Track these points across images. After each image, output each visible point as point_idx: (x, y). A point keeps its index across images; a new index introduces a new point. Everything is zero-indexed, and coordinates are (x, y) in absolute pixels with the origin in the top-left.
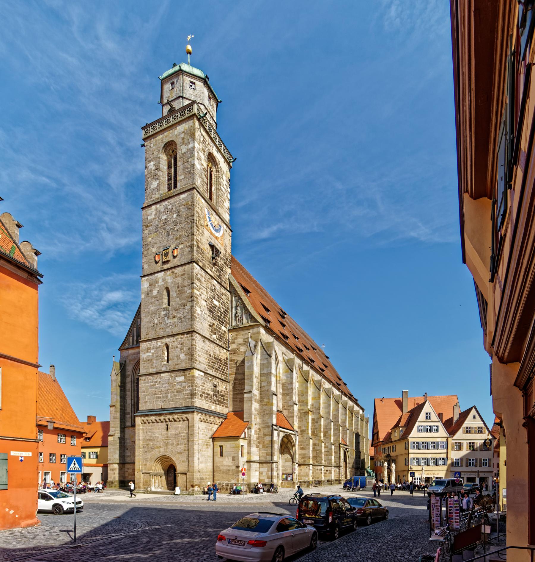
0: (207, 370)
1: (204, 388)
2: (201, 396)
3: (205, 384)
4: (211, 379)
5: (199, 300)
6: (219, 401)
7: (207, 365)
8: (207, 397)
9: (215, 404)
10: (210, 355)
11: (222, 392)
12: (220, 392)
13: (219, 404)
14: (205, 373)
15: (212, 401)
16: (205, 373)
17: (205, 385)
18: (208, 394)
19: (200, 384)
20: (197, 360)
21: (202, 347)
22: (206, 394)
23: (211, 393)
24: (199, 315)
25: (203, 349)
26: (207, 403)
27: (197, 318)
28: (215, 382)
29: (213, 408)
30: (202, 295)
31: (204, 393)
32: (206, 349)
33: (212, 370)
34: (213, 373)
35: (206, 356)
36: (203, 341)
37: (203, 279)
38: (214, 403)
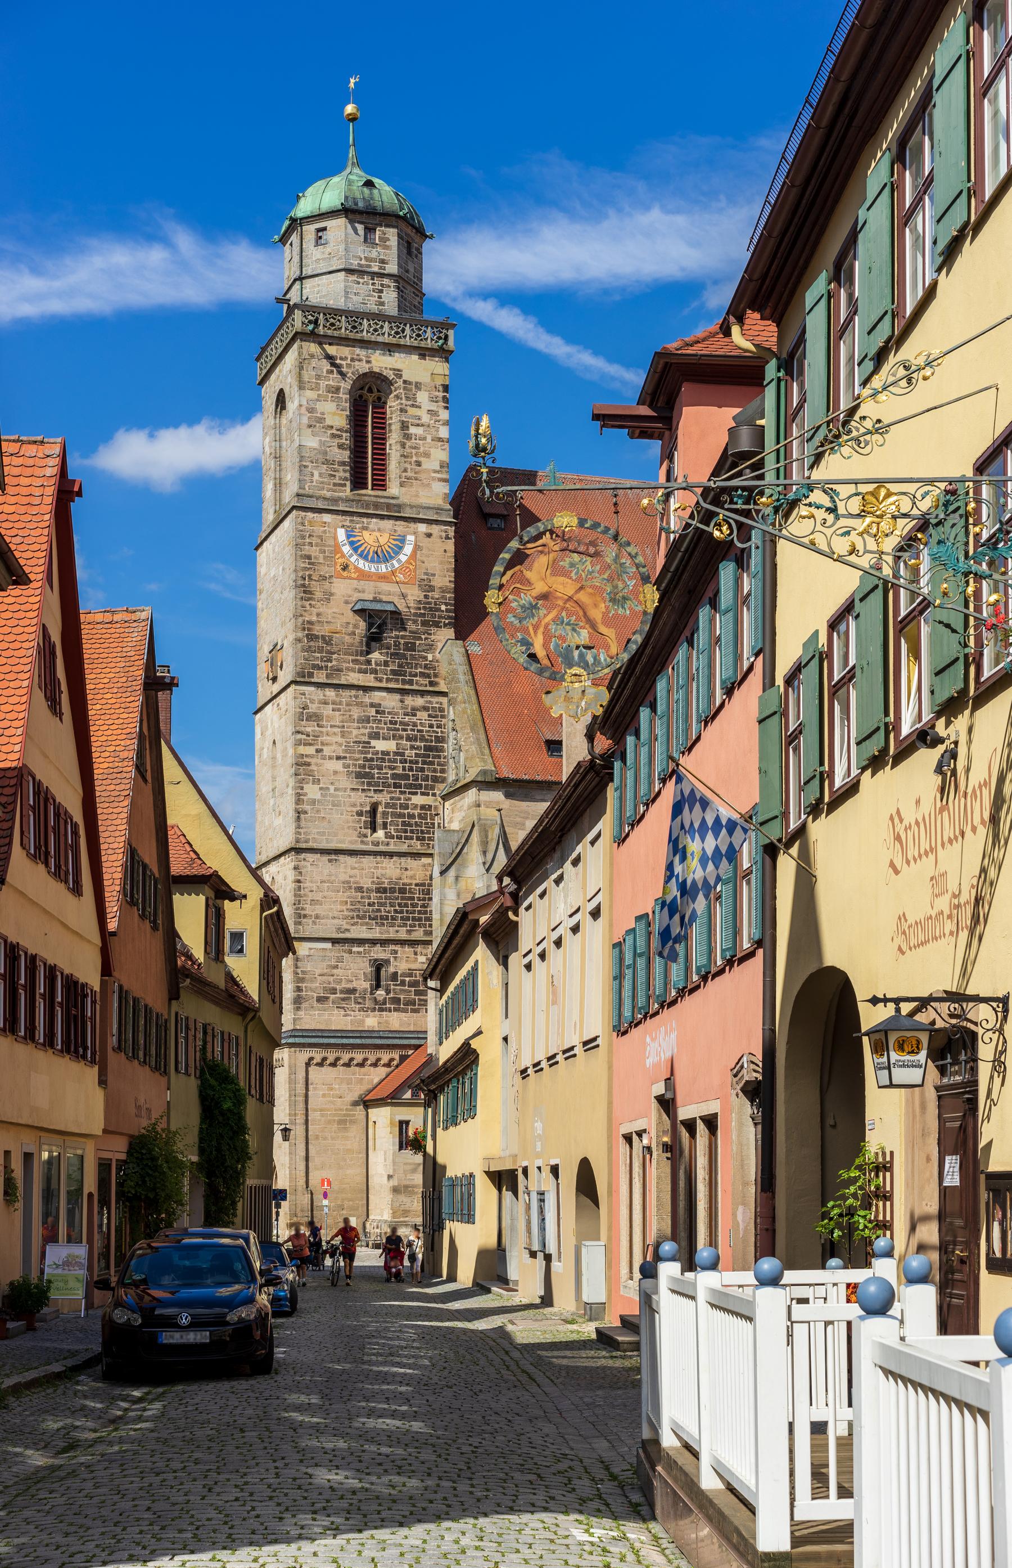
0: (348, 930)
1: (331, 979)
2: (320, 1000)
3: (336, 967)
4: (361, 949)
5: (313, 767)
6: (396, 1001)
7: (345, 918)
8: (343, 999)
9: (381, 1010)
10: (360, 889)
11: (410, 975)
12: (403, 975)
13: (395, 1010)
14: (335, 941)
15: (368, 1004)
16: (335, 941)
17: (335, 971)
18: (353, 991)
19: (318, 972)
20: (305, 916)
21: (324, 878)
22: (342, 992)
23: (364, 984)
24: (313, 802)
25: (329, 881)
26: (345, 1016)
27: (306, 812)
28: (379, 953)
29: (371, 1022)
30: (325, 748)
31: (334, 991)
32: (343, 877)
33: (367, 924)
34: (376, 933)
35: (342, 896)
36: (330, 861)
37: (327, 711)
38: (374, 1010)
